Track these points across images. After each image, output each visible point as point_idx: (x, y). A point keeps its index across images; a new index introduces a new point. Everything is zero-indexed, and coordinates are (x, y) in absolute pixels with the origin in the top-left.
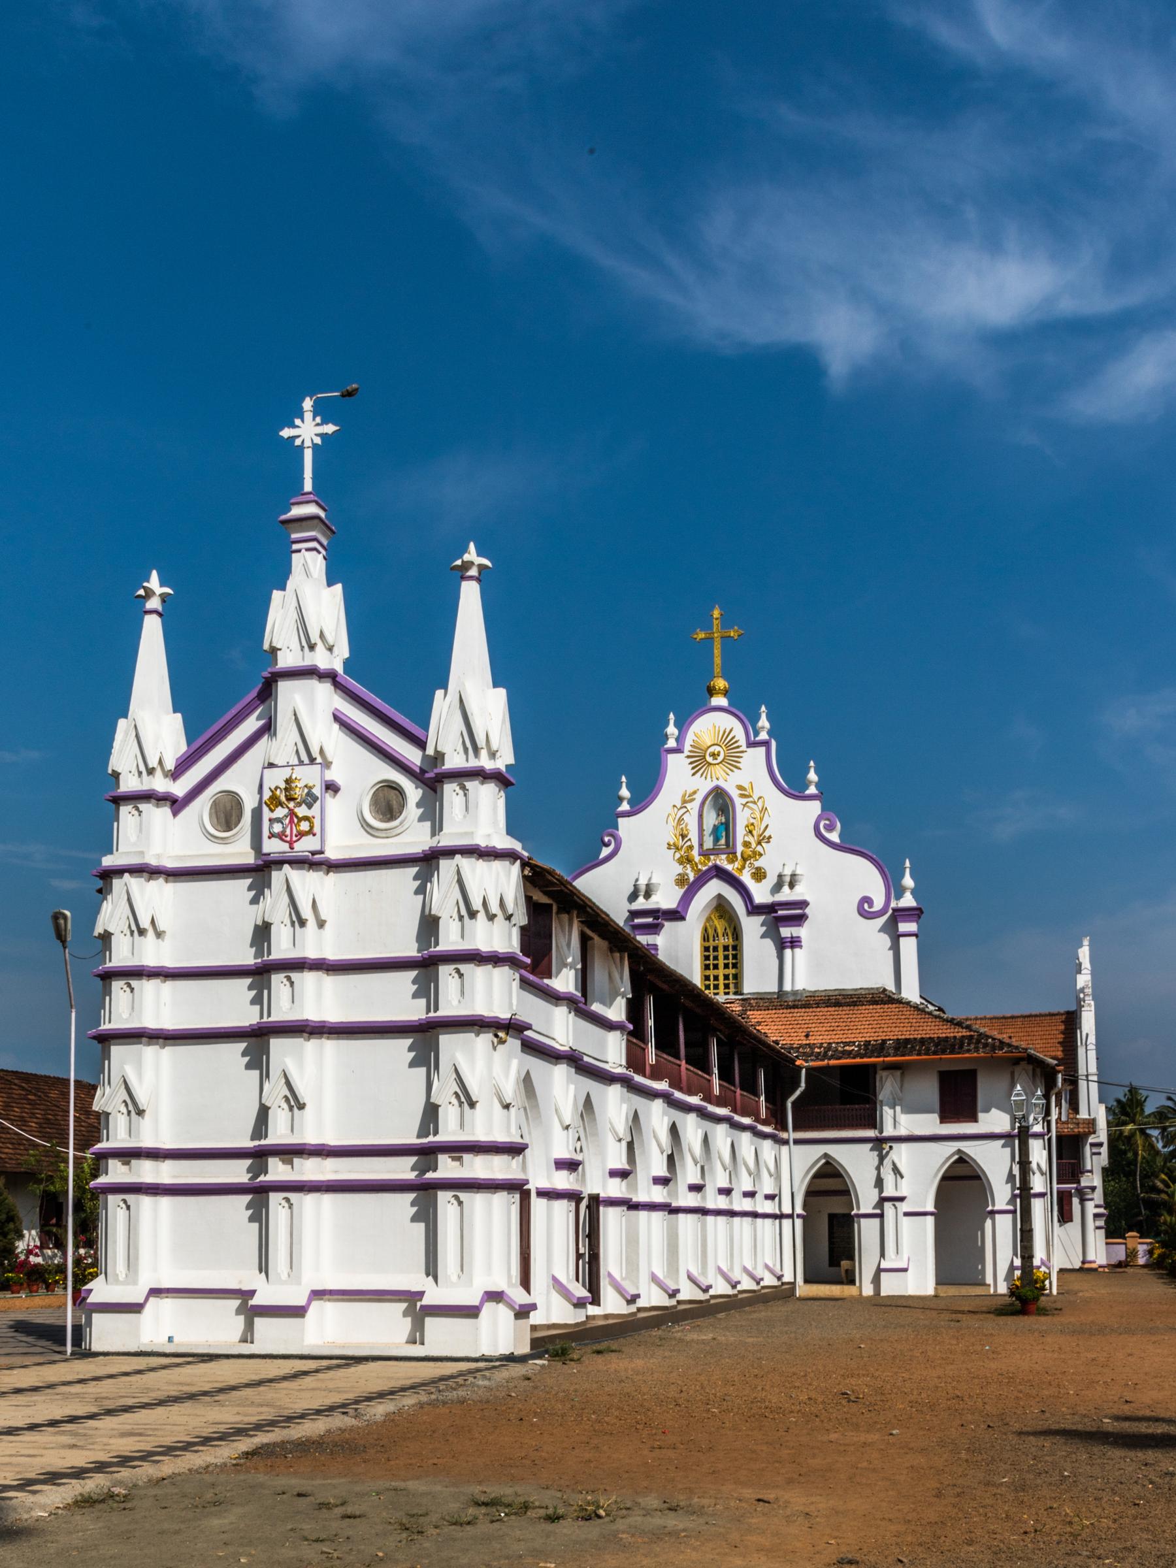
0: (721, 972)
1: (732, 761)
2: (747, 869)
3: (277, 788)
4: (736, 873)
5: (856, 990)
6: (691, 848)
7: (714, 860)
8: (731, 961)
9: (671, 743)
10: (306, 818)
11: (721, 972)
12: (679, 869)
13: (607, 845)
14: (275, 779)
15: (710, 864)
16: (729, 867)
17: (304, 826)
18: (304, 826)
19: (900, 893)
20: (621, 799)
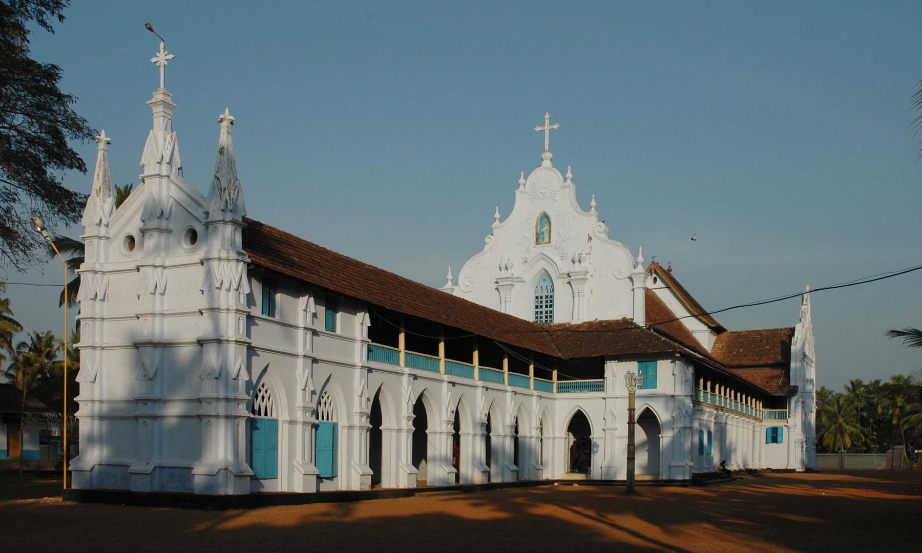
0: (544, 309)
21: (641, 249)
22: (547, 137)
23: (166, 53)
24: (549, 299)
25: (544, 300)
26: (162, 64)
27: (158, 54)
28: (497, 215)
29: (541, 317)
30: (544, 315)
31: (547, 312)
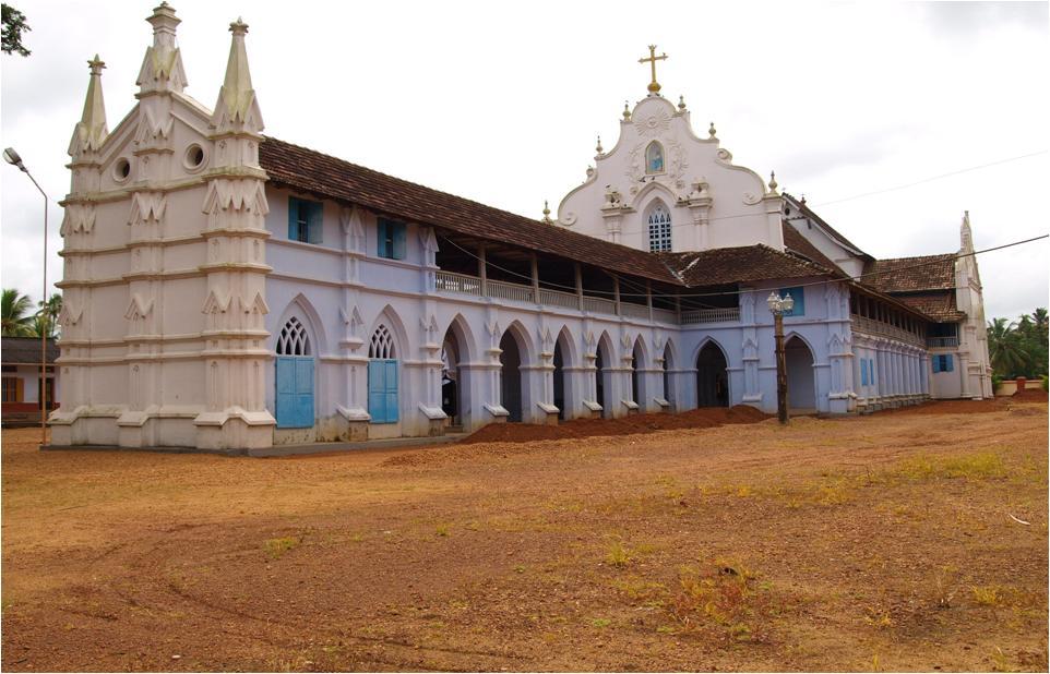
8: (666, 233)
11: (660, 239)
24: (666, 228)
29: (658, 247)
30: (661, 245)
31: (663, 242)
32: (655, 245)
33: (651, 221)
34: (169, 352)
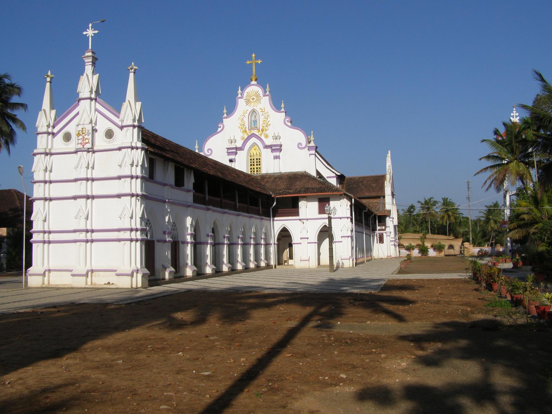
0: (255, 167)
1: (259, 100)
2: (263, 134)
3: (80, 130)
4: (259, 135)
5: (297, 172)
6: (246, 128)
7: (253, 132)
8: (258, 163)
9: (239, 96)
10: (87, 139)
11: (255, 167)
12: (242, 135)
13: (220, 127)
14: (80, 128)
15: (252, 133)
16: (257, 134)
17: (87, 141)
18: (87, 141)
19: (309, 142)
20: (224, 114)
21: (312, 132)
22: (254, 67)
23: (93, 29)
24: (258, 161)
25: (255, 161)
26: (90, 36)
27: (88, 30)
28: (225, 111)
29: (254, 171)
30: (255, 170)
31: (257, 168)
32: (252, 170)
33: (251, 156)
34: (96, 236)
